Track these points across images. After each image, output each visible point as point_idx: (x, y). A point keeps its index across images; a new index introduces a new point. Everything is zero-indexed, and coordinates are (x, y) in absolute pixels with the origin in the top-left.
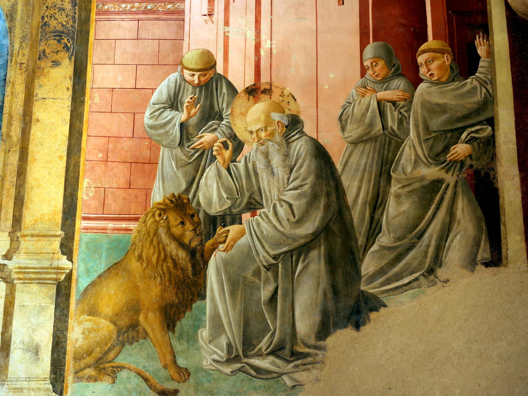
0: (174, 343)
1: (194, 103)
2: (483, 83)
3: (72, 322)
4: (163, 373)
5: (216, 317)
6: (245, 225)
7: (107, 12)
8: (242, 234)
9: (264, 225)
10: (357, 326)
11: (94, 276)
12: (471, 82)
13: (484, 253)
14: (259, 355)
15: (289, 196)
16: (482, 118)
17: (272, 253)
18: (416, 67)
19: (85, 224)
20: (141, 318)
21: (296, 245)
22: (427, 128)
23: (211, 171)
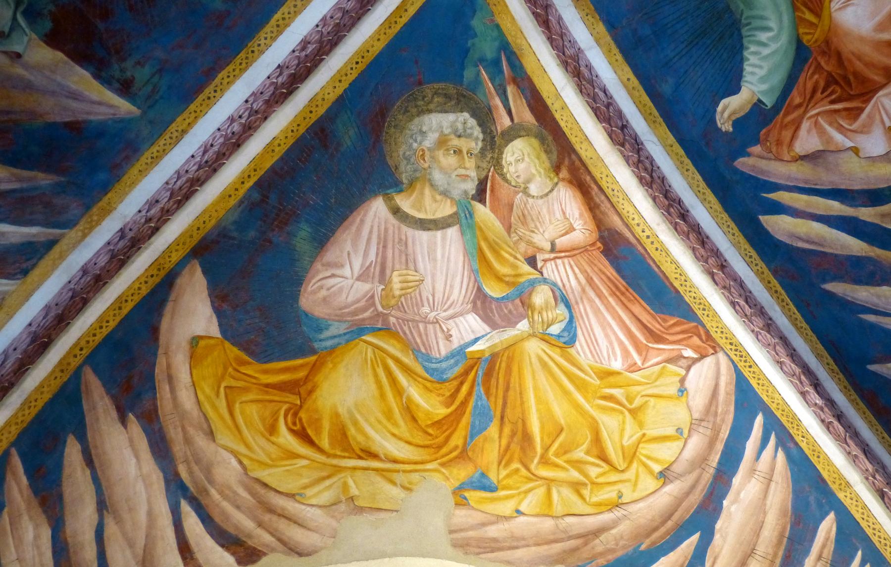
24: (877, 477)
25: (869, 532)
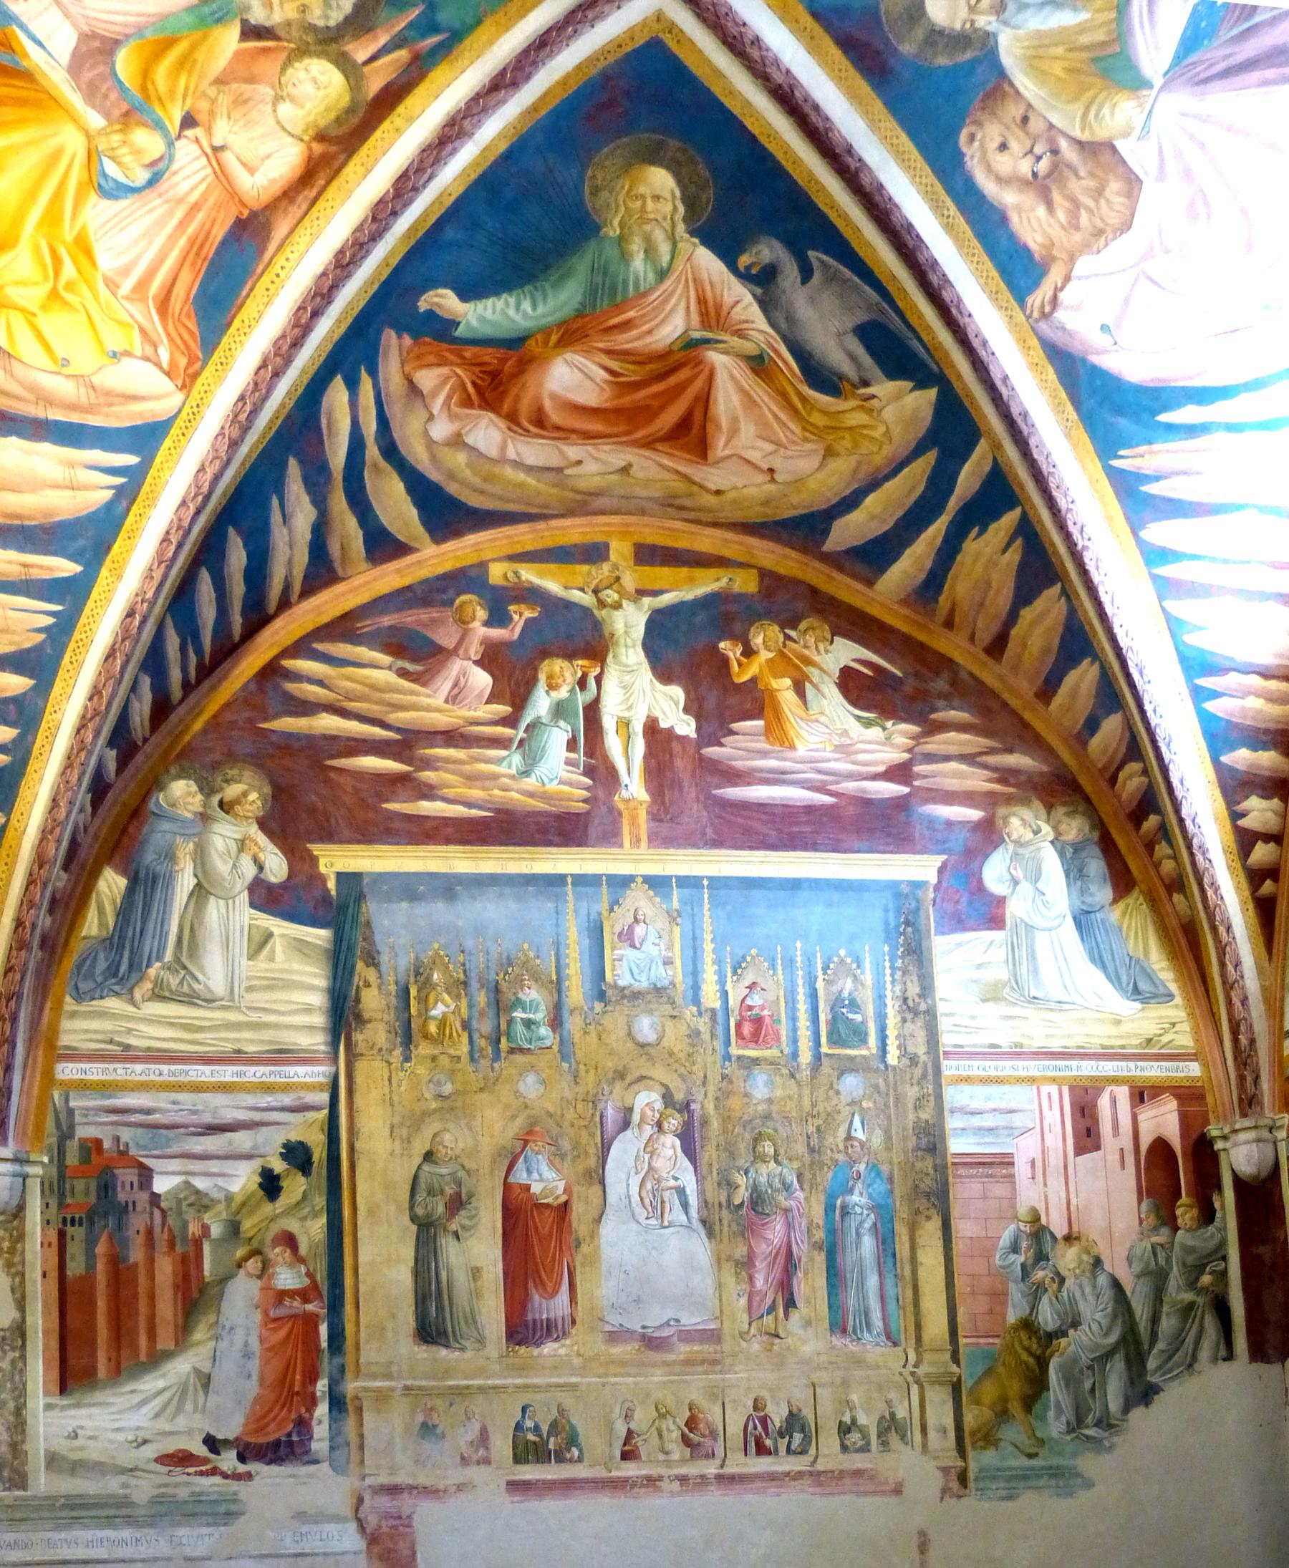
0: (1033, 1422)
1: (1029, 1248)
2: (1219, 1230)
3: (965, 1411)
4: (1027, 1442)
5: (1058, 1403)
6: (1071, 1338)
7: (961, 1176)
8: (1069, 1344)
9: (1083, 1337)
10: (1147, 1405)
11: (976, 1378)
12: (1211, 1228)
13: (1223, 1353)
14: (1087, 1427)
15: (1098, 1316)
16: (1219, 1255)
17: (1092, 1357)
18: (1175, 1218)
19: (965, 1340)
20: (1010, 1406)
21: (1104, 1351)
22: (1184, 1264)
23: (1045, 1300)
24: (145, 605)
25: (87, 611)
